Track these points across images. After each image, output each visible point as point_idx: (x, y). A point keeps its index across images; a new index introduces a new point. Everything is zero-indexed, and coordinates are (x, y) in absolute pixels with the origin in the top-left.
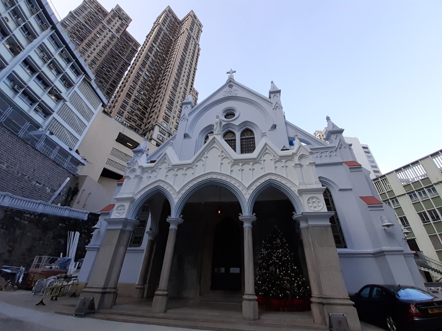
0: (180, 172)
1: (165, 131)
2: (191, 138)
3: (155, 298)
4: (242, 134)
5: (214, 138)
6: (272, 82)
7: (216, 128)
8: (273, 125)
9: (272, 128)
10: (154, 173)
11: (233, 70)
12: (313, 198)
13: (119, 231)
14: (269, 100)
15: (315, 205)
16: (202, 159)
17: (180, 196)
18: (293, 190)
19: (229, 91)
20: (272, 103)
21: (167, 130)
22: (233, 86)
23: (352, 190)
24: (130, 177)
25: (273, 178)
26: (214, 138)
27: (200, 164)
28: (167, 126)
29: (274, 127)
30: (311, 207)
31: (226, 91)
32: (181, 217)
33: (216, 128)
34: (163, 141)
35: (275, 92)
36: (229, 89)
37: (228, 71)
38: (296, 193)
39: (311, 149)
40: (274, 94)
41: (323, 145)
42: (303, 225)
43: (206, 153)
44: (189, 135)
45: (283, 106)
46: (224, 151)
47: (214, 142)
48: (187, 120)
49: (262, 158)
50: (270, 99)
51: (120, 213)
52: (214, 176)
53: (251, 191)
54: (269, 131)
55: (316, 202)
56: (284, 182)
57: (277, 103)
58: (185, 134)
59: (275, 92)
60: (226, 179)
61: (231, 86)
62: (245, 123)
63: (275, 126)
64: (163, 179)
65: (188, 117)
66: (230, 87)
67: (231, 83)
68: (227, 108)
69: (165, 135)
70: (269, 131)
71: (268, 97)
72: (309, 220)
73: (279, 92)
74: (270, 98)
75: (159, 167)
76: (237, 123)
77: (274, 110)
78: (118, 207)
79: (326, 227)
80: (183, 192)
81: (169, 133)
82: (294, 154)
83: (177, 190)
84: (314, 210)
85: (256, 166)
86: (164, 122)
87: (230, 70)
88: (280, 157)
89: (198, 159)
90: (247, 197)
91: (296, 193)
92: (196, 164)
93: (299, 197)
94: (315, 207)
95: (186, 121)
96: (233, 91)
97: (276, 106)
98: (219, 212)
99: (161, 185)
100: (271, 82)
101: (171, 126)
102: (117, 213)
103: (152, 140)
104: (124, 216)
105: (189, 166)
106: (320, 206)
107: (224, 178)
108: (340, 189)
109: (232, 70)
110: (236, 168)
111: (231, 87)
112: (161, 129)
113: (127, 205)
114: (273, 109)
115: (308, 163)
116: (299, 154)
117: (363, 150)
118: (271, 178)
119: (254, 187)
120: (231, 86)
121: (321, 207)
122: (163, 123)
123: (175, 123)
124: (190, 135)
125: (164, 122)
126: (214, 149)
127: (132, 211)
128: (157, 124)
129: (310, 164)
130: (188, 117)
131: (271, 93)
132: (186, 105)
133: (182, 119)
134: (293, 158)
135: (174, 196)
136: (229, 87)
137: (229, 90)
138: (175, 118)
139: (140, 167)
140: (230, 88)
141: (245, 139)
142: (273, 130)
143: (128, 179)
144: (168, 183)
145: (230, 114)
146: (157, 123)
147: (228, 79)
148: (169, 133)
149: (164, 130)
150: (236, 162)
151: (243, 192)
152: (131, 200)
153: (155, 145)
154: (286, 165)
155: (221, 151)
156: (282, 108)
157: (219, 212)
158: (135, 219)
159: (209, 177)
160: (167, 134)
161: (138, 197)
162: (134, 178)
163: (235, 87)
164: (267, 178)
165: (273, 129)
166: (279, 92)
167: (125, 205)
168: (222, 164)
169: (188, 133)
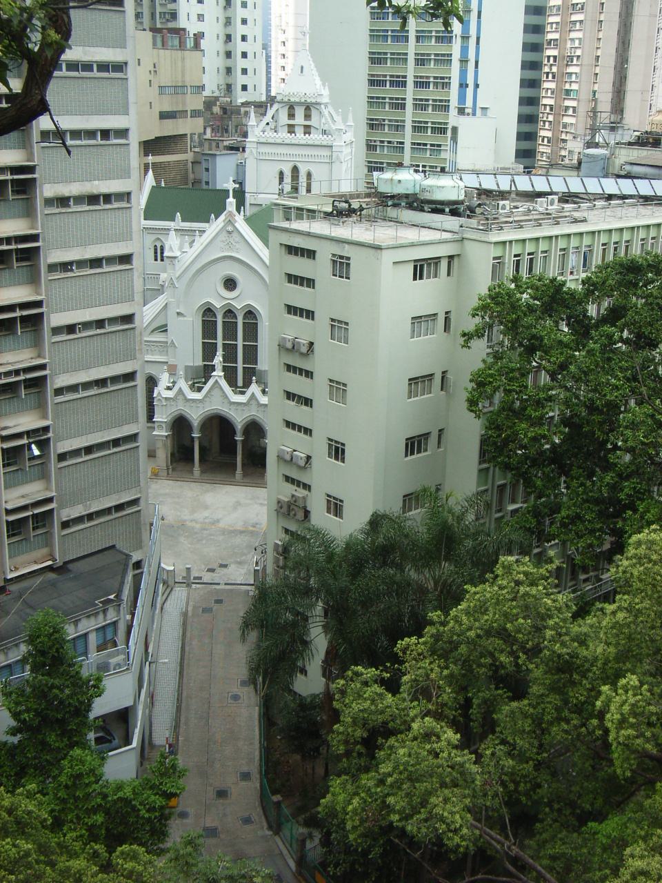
5: (216, 381)
26: (216, 381)
27: (207, 399)
31: (224, 239)
52: (219, 411)
89: (206, 396)
90: (239, 427)
119: (244, 422)
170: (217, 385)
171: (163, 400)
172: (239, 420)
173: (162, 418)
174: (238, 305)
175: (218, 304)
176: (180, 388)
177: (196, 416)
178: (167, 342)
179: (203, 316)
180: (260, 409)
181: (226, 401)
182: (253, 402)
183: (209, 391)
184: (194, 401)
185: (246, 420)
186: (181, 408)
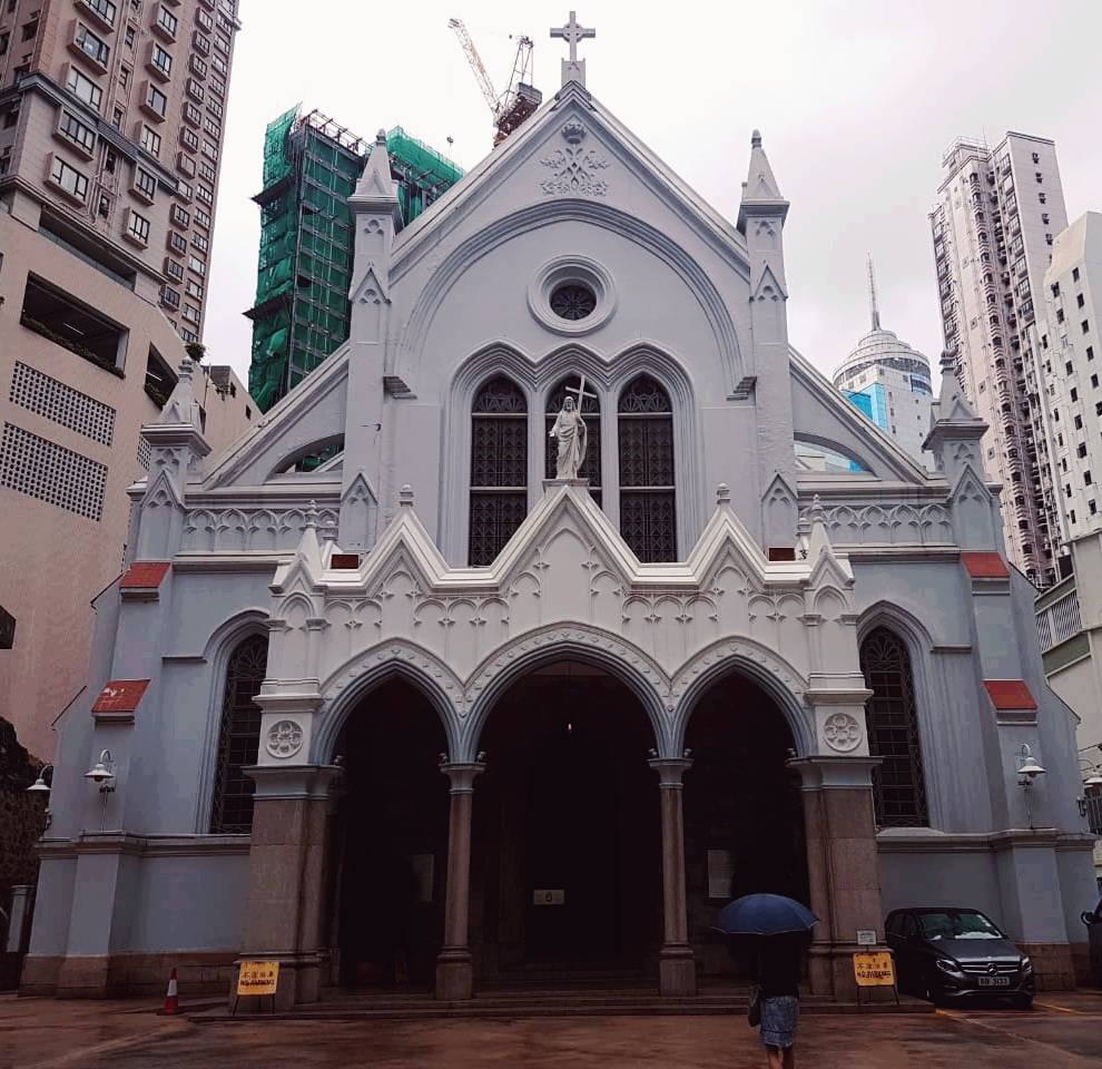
0: (462, 614)
1: (87, 129)
2: (415, 398)
4: (624, 401)
6: (756, 141)
7: (568, 452)
8: (745, 379)
9: (740, 388)
10: (368, 610)
11: (584, 22)
12: (839, 716)
13: (300, 805)
15: (844, 736)
16: (531, 570)
17: (474, 695)
18: (793, 691)
19: (570, 164)
20: (748, 269)
21: (97, 120)
22: (583, 135)
23: (970, 653)
24: (289, 624)
25: (742, 650)
27: (524, 588)
28: (96, 92)
29: (749, 387)
30: (832, 740)
31: (556, 158)
32: (480, 756)
33: (568, 452)
34: (80, 197)
35: (765, 213)
36: (568, 150)
37: (561, 23)
38: (799, 698)
39: (855, 560)
40: (760, 220)
41: (914, 480)
42: (809, 785)
43: (541, 550)
45: (789, 290)
46: (599, 549)
47: (566, 509)
48: (389, 302)
49: (716, 585)
50: (737, 236)
52: (574, 636)
53: (681, 689)
54: (728, 399)
55: (846, 729)
56: (770, 665)
57: (767, 267)
58: (385, 378)
59: (765, 213)
60: (611, 646)
61: (573, 137)
63: (754, 385)
65: (390, 287)
66: (571, 142)
68: (562, 263)
69: (85, 159)
70: (728, 399)
71: (735, 226)
72: (825, 776)
73: (780, 210)
74: (741, 228)
75: (384, 590)
76: (606, 348)
78: (275, 729)
79: (861, 791)
80: (483, 681)
81: (112, 146)
82: (805, 583)
83: (464, 679)
84: (840, 749)
85: (700, 611)
86: (79, 73)
87: (567, 21)
88: (767, 586)
89: (517, 572)
91: (799, 698)
92: (514, 590)
93: (806, 711)
94: (842, 742)
95: (384, 306)
96: (585, 168)
97: (764, 286)
98: (570, 726)
99: (404, 654)
100: (754, 140)
101: (119, 94)
102: (274, 748)
103: (18, 200)
104: (301, 760)
105: (492, 595)
106: (853, 740)
107: (603, 643)
108: (935, 648)
109: (578, 21)
110: (638, 611)
111: (577, 142)
112: (63, 120)
113: (306, 722)
114: (751, 299)
115: (838, 617)
116: (819, 586)
118: (738, 652)
119: (690, 678)
120: (573, 137)
121: (855, 744)
122: (72, 76)
123: (139, 76)
124: (409, 387)
125: (79, 73)
126: (566, 535)
127: (320, 738)
128: (34, 89)
129: (845, 618)
130: (390, 287)
131: (748, 210)
132: (372, 217)
133: (362, 295)
134: (802, 595)
135: (454, 695)
136: (565, 135)
137: (567, 155)
138: (140, 42)
139: (322, 590)
140: (574, 148)
141: (636, 420)
142: (746, 398)
143: (284, 630)
144: (429, 653)
145: (574, 294)
146: (37, 80)
148: (107, 143)
149: (79, 124)
150: (638, 593)
151: (662, 690)
152: (314, 705)
153: (36, 225)
154: (781, 614)
155: (591, 549)
156: (785, 298)
157: (570, 726)
158: (332, 763)
159: (558, 636)
160: (99, 156)
162: (301, 629)
163: (591, 143)
164: (727, 652)
165: (745, 395)
166: (780, 210)
167: (302, 727)
169: (401, 378)
170: (567, 523)
174: (606, 348)
175: (536, 348)
176: (402, 544)
178: (339, 495)
179: (475, 408)
180: (762, 609)
181: (606, 587)
182: (730, 583)
184: (460, 595)
185: (701, 667)
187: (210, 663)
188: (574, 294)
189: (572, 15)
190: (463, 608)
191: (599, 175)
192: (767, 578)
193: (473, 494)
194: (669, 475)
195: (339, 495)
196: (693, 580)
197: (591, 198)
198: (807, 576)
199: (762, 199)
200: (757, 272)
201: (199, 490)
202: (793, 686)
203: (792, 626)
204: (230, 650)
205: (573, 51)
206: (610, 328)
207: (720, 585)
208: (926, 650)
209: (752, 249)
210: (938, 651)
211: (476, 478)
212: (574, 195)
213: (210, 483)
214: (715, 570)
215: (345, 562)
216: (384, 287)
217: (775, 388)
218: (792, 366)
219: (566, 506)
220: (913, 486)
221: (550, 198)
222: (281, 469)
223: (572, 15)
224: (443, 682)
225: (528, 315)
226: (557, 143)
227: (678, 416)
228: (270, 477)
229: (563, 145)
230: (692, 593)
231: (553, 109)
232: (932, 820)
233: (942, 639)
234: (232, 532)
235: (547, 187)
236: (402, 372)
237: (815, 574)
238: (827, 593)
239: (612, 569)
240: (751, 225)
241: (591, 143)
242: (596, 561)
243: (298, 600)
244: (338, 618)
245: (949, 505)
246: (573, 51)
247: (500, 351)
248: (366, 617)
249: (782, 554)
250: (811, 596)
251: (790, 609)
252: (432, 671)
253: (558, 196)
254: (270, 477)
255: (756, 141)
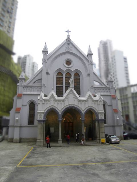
0: (59, 103)
3: (59, 141)
4: (74, 76)
5: (71, 89)
6: (89, 46)
10: (49, 102)
11: (70, 31)
12: (101, 115)
14: (87, 57)
16: (67, 98)
20: (88, 61)
22: (70, 44)
26: (71, 89)
29: (89, 75)
37: (67, 30)
44: (49, 73)
50: (87, 57)
51: (41, 118)
52: (72, 105)
53: (84, 112)
61: (68, 44)
62: (77, 70)
64: (53, 105)
67: (68, 41)
70: (87, 76)
73: (92, 54)
74: (88, 56)
76: (73, 69)
77: (90, 65)
85: (87, 103)
89: (66, 98)
99: (53, 107)
104: (42, 119)
105: (63, 101)
107: (76, 106)
110: (80, 103)
117: (123, 60)
119: (85, 110)
120: (68, 44)
135: (59, 112)
145: (68, 62)
147: (66, 38)
151: (82, 112)
161: (46, 111)
163: (70, 45)
168: (75, 101)
170: (71, 92)
171: (43, 101)
172: (83, 108)
173: (42, 110)
174: (73, 69)
175: (64, 69)
176: (53, 94)
177: (60, 108)
178: (41, 86)
179: (57, 76)
180: (93, 103)
181: (76, 100)
182: (90, 100)
183: (67, 95)
186: (52, 104)
187: (27, 106)
188: (68, 62)
189: (68, 29)
190: (60, 102)
191: (72, 49)
192: (94, 99)
193: (57, 86)
194: (79, 85)
195: (41, 86)
196: (86, 99)
197: (71, 51)
198: (98, 99)
199: (90, 53)
200: (90, 61)
201: (25, 85)
202: (96, 111)
203: (96, 105)
204: (29, 104)
205: (68, 34)
206: (73, 67)
207: (89, 100)
208: (107, 105)
209: (89, 59)
210: (108, 106)
211: (57, 84)
212: (69, 51)
213: (26, 84)
214: (88, 98)
215: (45, 96)
216: (47, 61)
217: (92, 75)
218: (94, 73)
219: (71, 90)
220: (106, 87)
221: (66, 51)
222: (34, 83)
223: (68, 29)
224: (58, 110)
225: (63, 65)
226: (66, 45)
227: (80, 77)
228: (33, 84)
229: (67, 45)
230: (85, 101)
231: (66, 41)
232: (107, 123)
233: (109, 105)
234: (29, 91)
235: (66, 50)
236: (49, 72)
237: (99, 99)
238: (100, 101)
239: (77, 98)
240: (89, 56)
241: (70, 45)
242: (75, 97)
243: (41, 101)
244: (46, 103)
245: (110, 89)
246: (68, 34)
247: (60, 69)
248: (49, 103)
249: (95, 96)
250: (99, 102)
251: (96, 103)
252: (56, 109)
253: (67, 51)
254: (33, 84)
255: (89, 46)
